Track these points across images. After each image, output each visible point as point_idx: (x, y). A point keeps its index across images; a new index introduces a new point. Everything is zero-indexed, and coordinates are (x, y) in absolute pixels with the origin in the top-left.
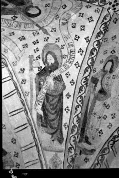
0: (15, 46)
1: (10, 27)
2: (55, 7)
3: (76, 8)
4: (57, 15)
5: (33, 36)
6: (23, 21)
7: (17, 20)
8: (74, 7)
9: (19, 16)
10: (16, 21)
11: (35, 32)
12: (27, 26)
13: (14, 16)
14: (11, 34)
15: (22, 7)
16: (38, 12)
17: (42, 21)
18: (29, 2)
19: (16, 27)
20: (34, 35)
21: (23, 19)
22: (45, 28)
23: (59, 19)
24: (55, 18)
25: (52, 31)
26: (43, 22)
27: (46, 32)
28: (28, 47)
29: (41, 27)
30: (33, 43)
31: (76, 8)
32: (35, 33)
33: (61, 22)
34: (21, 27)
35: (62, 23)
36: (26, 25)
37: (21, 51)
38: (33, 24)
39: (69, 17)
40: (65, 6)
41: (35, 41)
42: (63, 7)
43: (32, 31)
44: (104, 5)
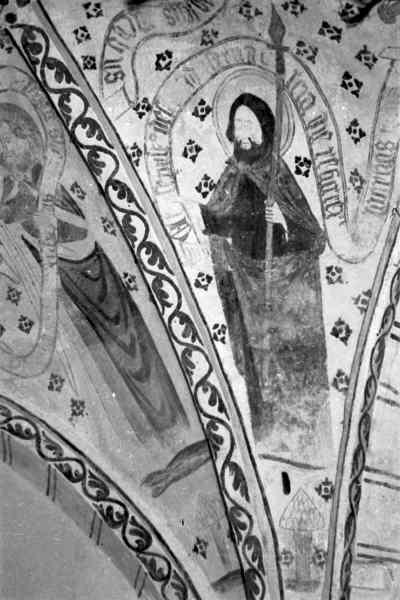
0: (387, 90)
1: (337, 156)
2: (188, 82)
3: (134, 30)
4: (204, 47)
5: (320, 53)
6: (299, 129)
7: (305, 154)
8: (140, 35)
9: (289, 160)
10: (311, 151)
11: (304, 58)
12: (306, 96)
13: (298, 172)
14: (357, 135)
15: (257, 179)
16: (245, 113)
17: (260, 67)
18: (231, 176)
19: (327, 136)
20: (315, 51)
21: (292, 132)
22: (266, 37)
23: (209, 27)
24: (215, 41)
25: (258, 13)
26: (258, 63)
27: (277, 26)
28: (365, 47)
29: (274, 52)
30: (338, 38)
31: (134, 30)
32: (306, 55)
33: (209, 14)
34: (320, 117)
35: (207, 10)
36: (305, 105)
37: (393, 62)
38: (288, 87)
39: (174, 10)
40: (161, 62)
41: (329, 35)
42: (168, 60)
43: (307, 69)
44: (32, 28)
